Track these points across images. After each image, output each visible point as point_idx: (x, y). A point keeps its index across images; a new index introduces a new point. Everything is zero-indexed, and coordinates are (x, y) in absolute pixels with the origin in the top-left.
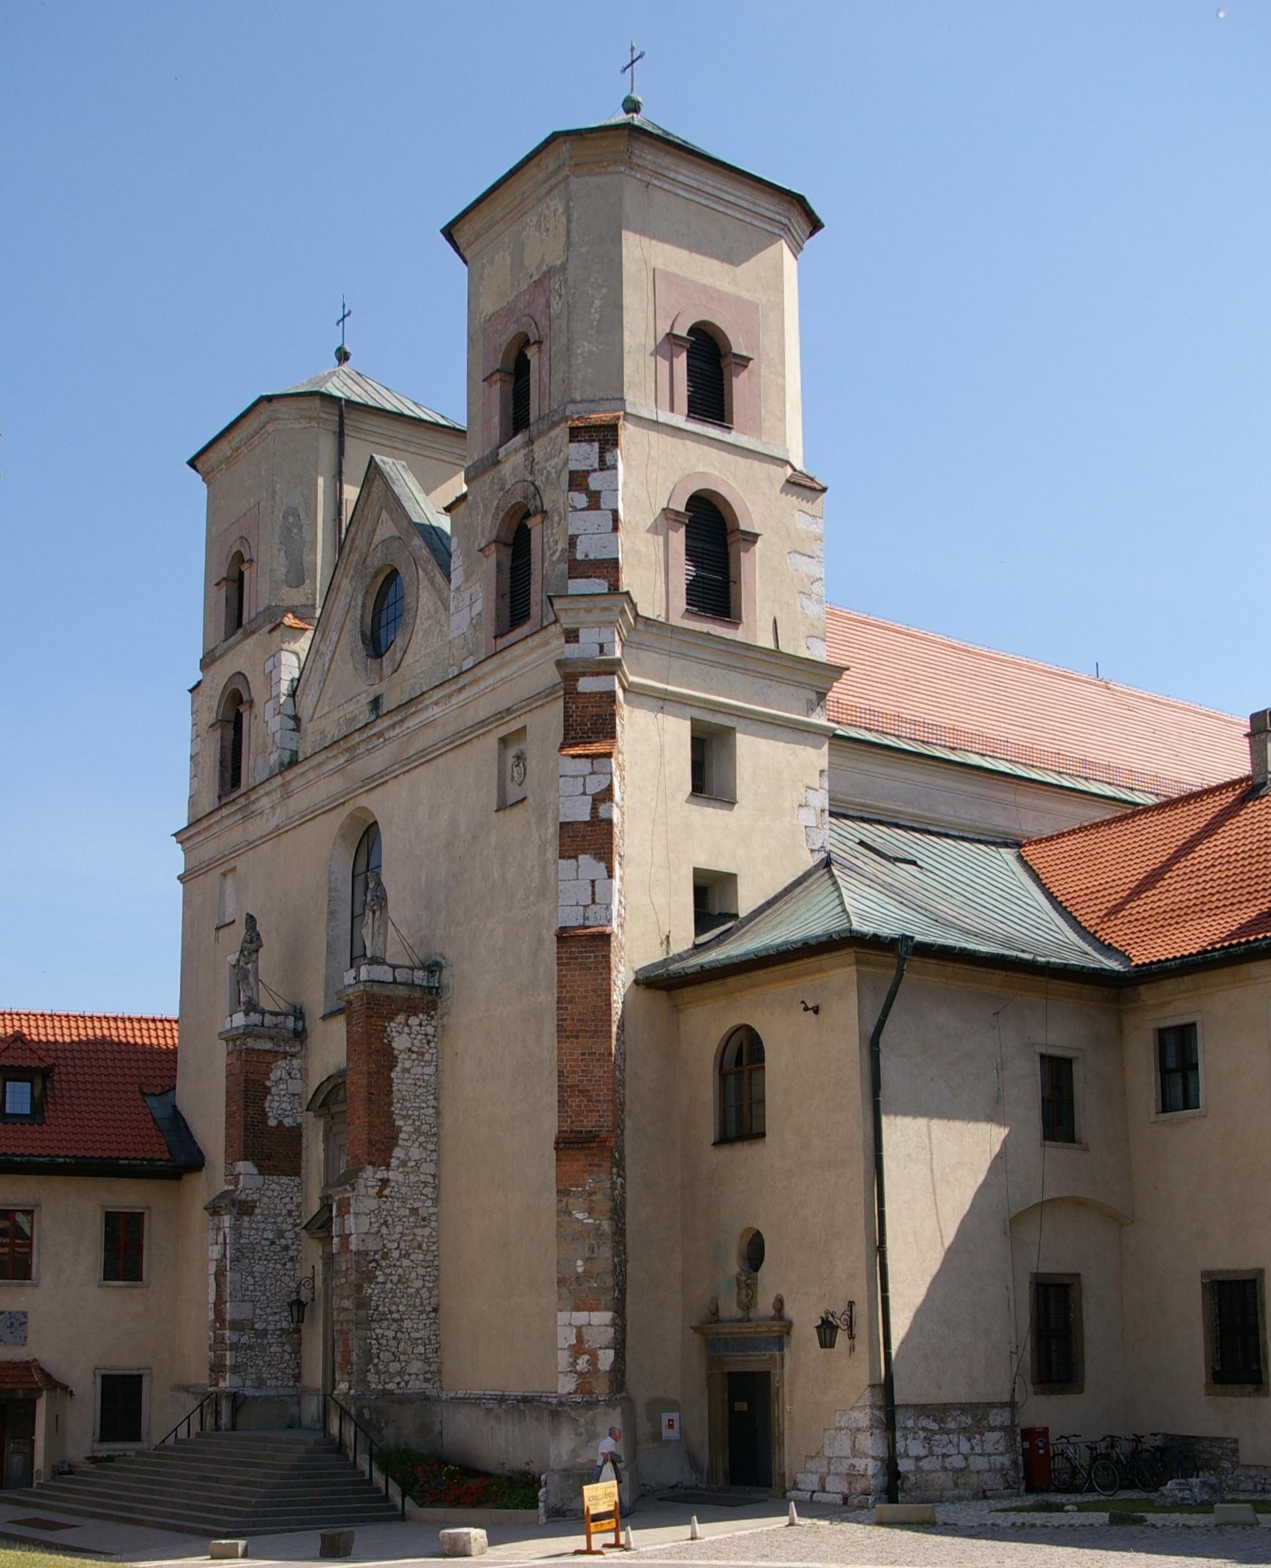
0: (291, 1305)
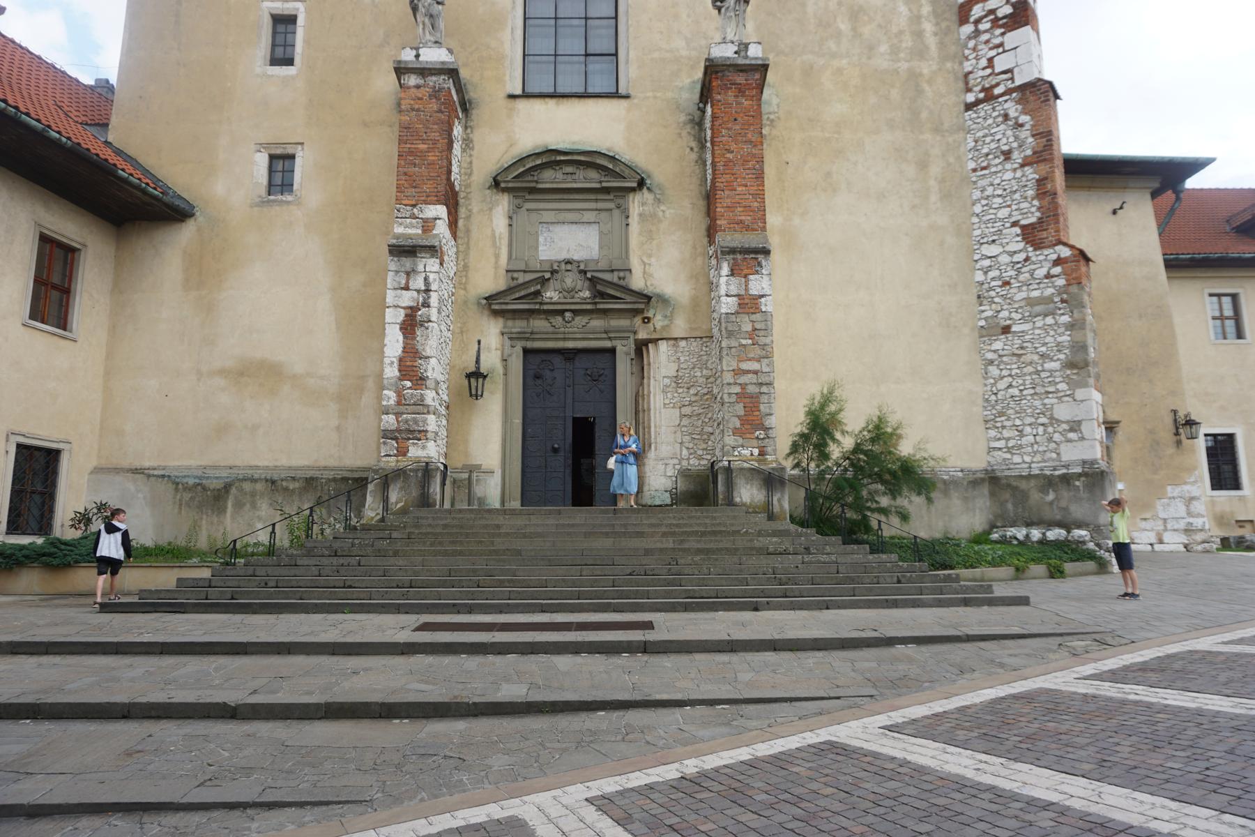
0: (469, 376)
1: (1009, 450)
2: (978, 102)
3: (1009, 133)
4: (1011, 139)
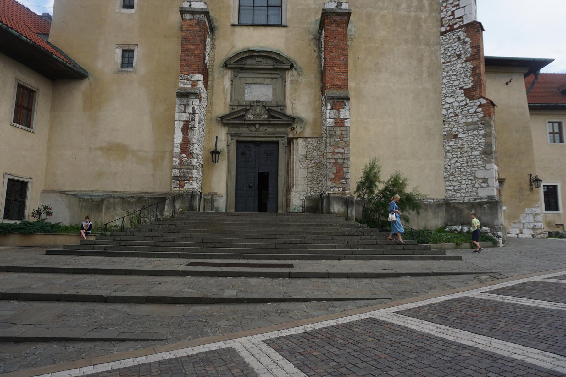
0: (212, 153)
1: (455, 191)
2: (446, 32)
3: (460, 46)
4: (461, 49)
